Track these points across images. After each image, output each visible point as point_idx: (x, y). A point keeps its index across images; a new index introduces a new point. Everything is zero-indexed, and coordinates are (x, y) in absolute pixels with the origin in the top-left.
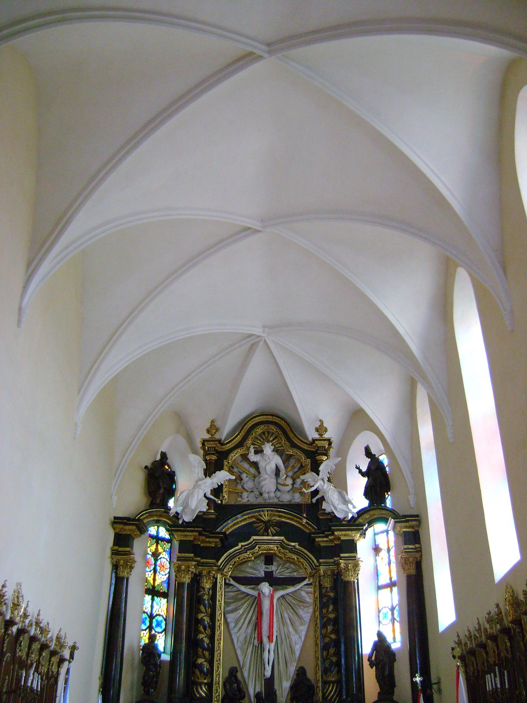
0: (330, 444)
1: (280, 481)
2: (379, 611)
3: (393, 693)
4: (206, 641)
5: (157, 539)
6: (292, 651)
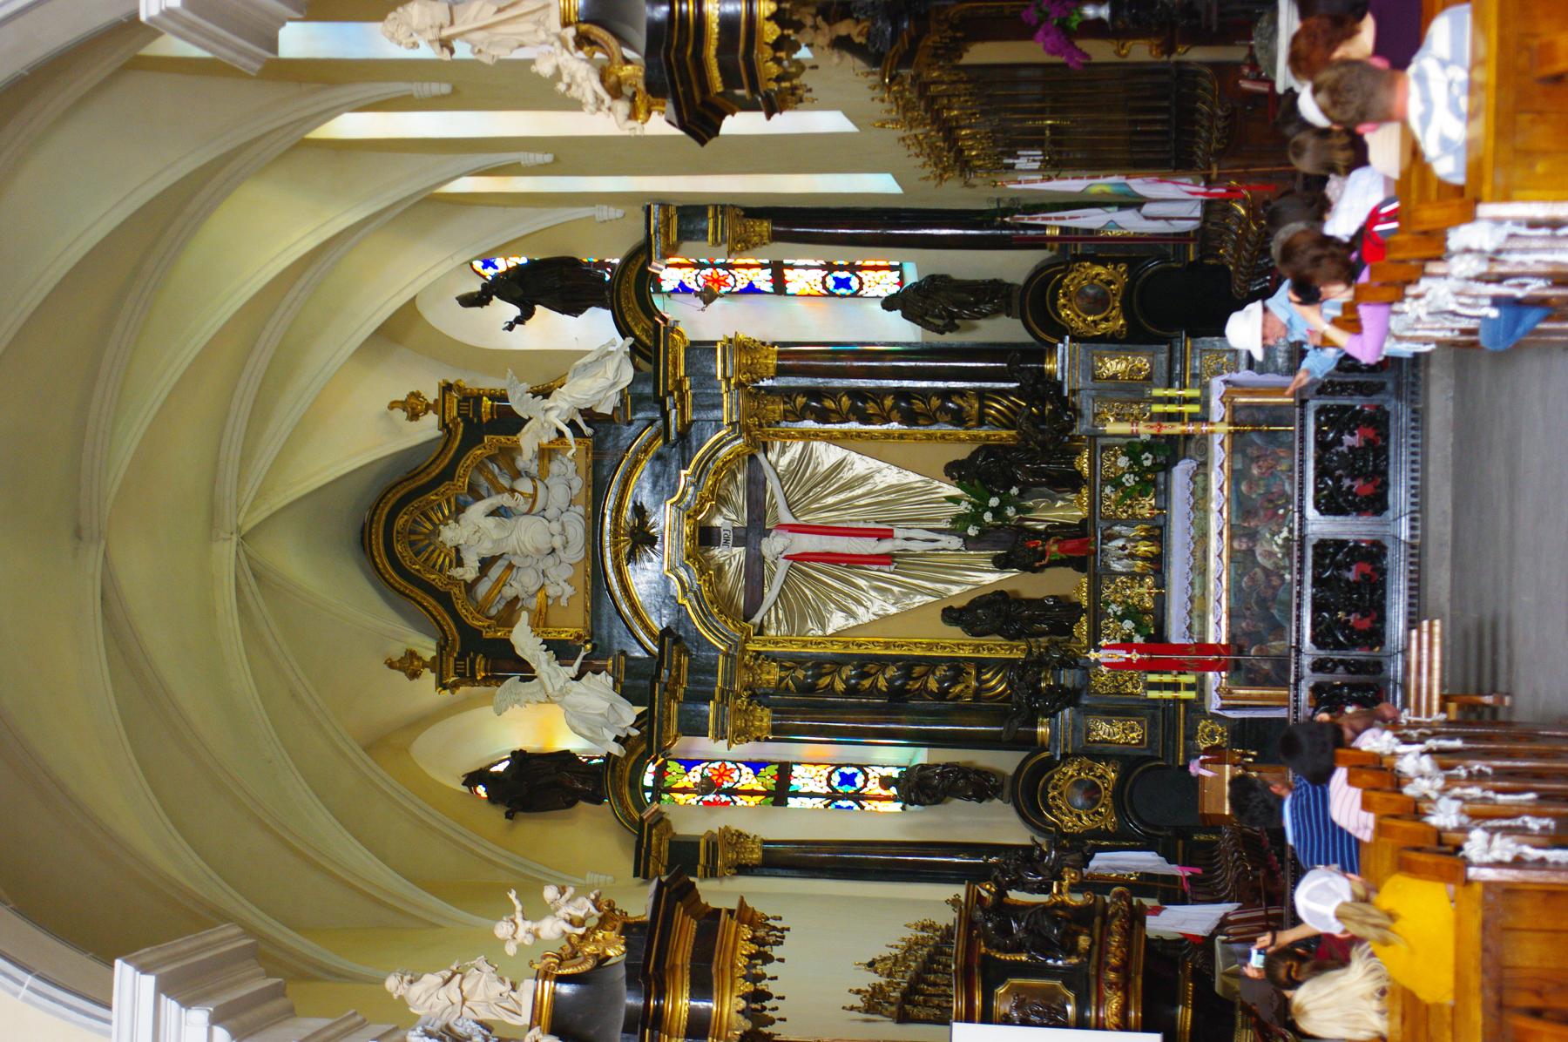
0: (447, 388)
1: (525, 508)
2: (832, 294)
3: (1010, 285)
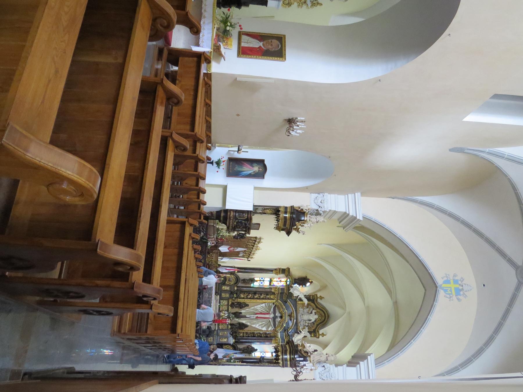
4: (256, 297)
5: (286, 282)
6: (254, 324)
